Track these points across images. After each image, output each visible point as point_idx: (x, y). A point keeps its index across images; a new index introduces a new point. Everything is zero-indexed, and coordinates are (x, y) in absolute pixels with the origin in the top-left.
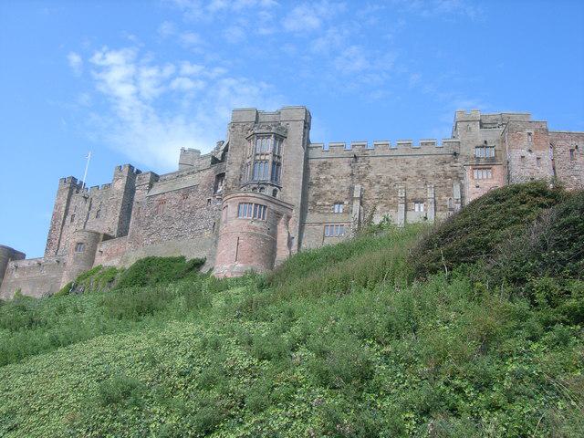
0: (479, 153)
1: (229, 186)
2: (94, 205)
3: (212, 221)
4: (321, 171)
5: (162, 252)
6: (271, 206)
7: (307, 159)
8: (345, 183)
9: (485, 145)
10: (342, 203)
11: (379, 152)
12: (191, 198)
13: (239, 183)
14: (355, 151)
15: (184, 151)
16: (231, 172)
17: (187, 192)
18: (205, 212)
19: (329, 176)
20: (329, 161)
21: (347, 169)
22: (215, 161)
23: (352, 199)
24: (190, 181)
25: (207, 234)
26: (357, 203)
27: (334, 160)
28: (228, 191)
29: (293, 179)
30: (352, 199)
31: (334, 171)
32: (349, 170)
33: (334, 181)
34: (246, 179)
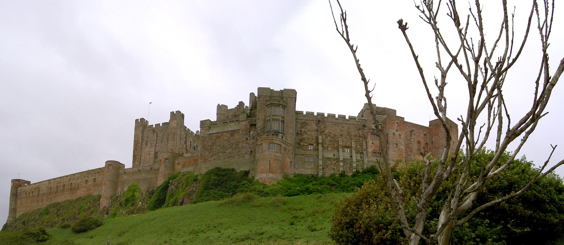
1: (259, 132)
3: (250, 150)
4: (302, 127)
5: (223, 164)
8: (314, 134)
10: (313, 145)
11: (330, 120)
14: (319, 118)
18: (245, 145)
19: (306, 130)
20: (306, 122)
21: (315, 127)
25: (247, 157)
27: (309, 122)
29: (291, 131)
31: (309, 127)
32: (315, 128)
33: (309, 133)
34: (267, 129)
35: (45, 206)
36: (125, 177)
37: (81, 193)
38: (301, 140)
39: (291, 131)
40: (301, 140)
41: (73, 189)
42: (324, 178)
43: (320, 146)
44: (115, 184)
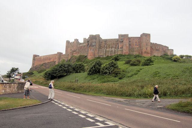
0: (121, 40)
2: (72, 45)
5: (82, 54)
6: (95, 49)
7: (99, 42)
9: (122, 39)
12: (85, 47)
13: (91, 45)
15: (84, 39)
16: (90, 44)
17: (84, 46)
22: (88, 42)
23: (105, 47)
24: (84, 45)
26: (105, 48)
28: (89, 47)
30: (105, 47)
35: (42, 63)
36: (62, 56)
37: (52, 60)
38: (101, 47)
39: (98, 45)
40: (101, 47)
41: (50, 59)
42: (109, 57)
43: (105, 48)
44: (59, 58)
